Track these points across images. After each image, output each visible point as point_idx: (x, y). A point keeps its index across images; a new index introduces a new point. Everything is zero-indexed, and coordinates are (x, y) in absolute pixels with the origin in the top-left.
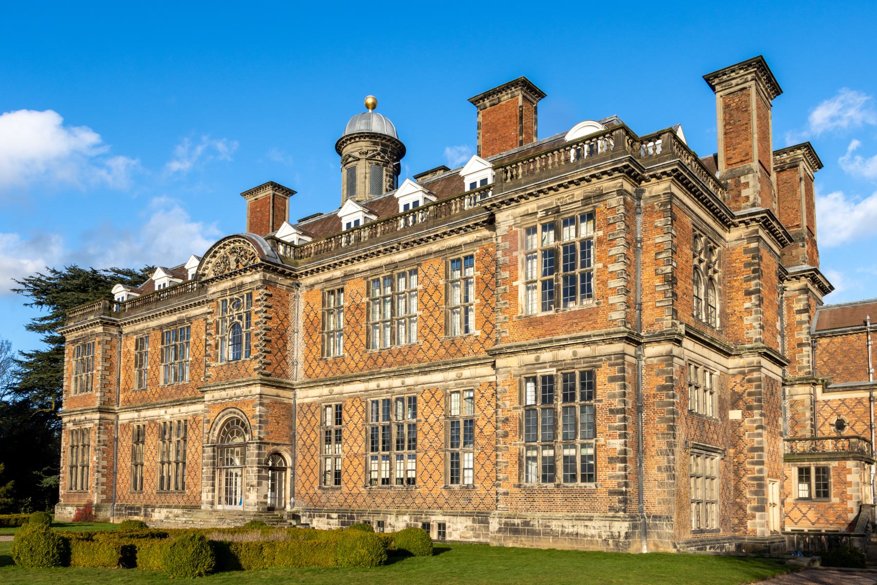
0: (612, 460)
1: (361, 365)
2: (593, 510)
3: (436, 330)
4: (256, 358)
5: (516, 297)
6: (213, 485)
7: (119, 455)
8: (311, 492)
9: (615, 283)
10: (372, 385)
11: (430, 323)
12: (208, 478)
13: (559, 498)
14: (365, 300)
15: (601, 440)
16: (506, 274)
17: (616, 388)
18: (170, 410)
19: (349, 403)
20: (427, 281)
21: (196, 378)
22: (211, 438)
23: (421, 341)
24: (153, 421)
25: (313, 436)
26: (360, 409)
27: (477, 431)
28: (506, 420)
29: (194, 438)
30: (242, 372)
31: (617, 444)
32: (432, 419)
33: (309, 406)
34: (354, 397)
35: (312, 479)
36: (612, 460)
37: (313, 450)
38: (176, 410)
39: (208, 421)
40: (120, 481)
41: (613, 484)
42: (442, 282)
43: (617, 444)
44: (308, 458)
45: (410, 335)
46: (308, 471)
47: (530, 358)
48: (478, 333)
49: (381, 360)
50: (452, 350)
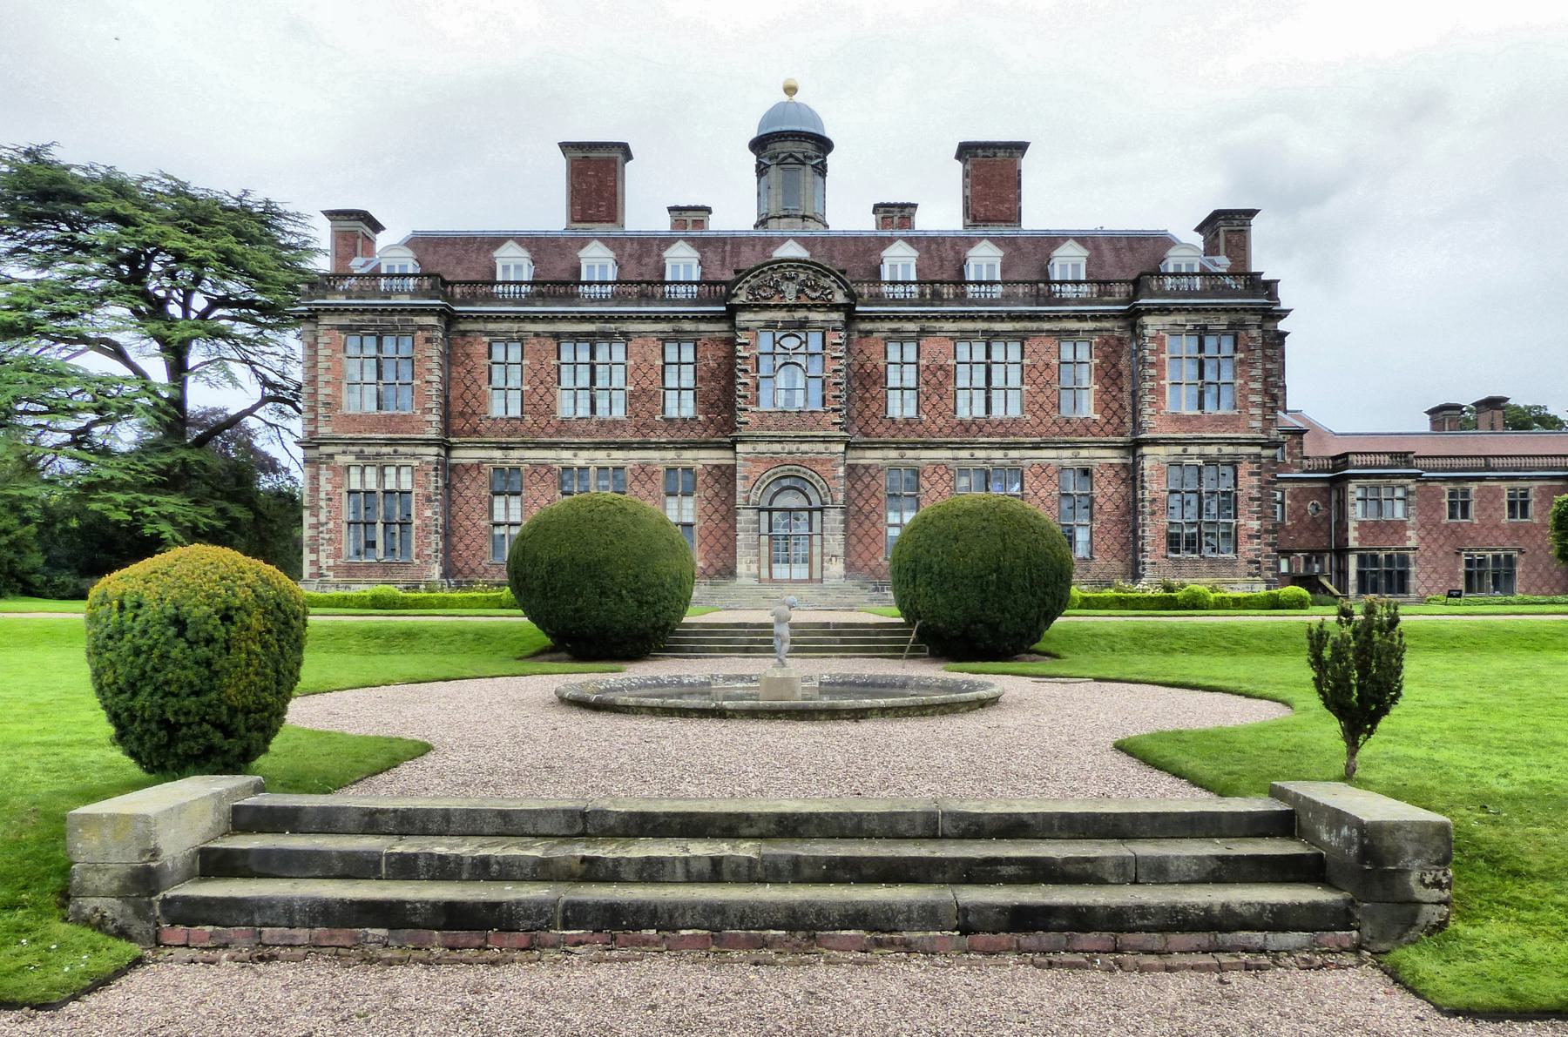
0: (1250, 537)
1: (946, 431)
2: (1235, 575)
3: (1048, 407)
4: (834, 410)
5: (1163, 394)
6: (758, 555)
7: (454, 509)
8: (873, 563)
9: (1253, 398)
10: (965, 454)
11: (1040, 398)
12: (748, 546)
13: (1204, 566)
14: (951, 362)
15: (1242, 522)
16: (1153, 372)
17: (1255, 480)
18: (584, 454)
19: (930, 470)
20: (1035, 357)
21: (644, 414)
22: (752, 498)
23: (1029, 417)
24: (543, 465)
25: (873, 502)
26: (946, 477)
27: (1096, 507)
28: (1154, 500)
29: (643, 492)
30: (809, 423)
31: (1255, 525)
32: (1042, 493)
33: (867, 468)
34: (937, 466)
35: (873, 548)
36: (1250, 537)
37: (874, 517)
38: (601, 454)
39: (746, 478)
40: (461, 546)
41: (1251, 555)
42: (1055, 362)
43: (1255, 525)
44: (867, 524)
45: (1008, 407)
46: (867, 540)
47: (1179, 450)
48: (1098, 417)
49: (974, 428)
50: (1067, 429)
